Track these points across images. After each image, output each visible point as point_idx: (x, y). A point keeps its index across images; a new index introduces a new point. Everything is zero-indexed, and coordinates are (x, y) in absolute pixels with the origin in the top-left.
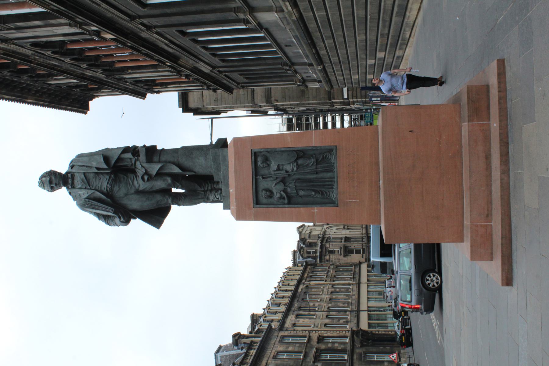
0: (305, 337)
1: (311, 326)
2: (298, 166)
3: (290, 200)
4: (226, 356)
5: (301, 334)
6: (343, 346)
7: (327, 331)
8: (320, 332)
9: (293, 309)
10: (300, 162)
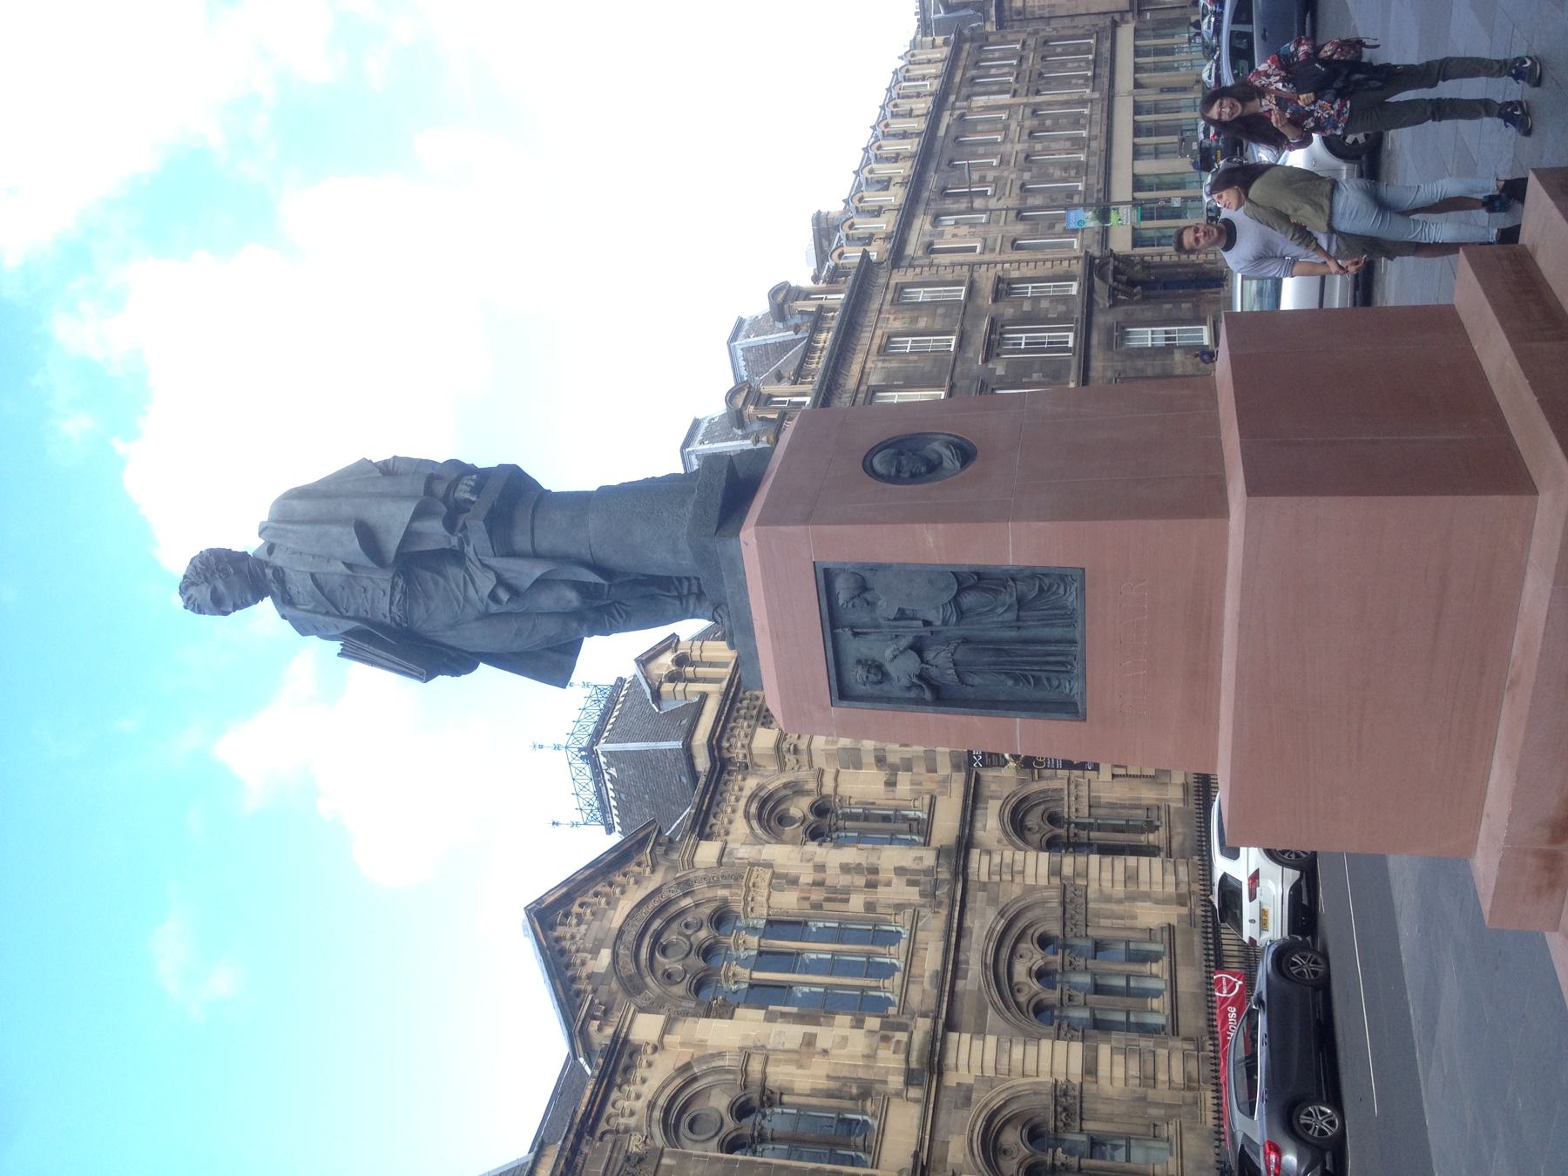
0: (959, 283)
1: (973, 249)
2: (961, 614)
3: (935, 693)
4: (758, 348)
5: (949, 277)
6: (1062, 308)
7: (1019, 262)
8: (999, 267)
9: (925, 195)
10: (969, 600)
